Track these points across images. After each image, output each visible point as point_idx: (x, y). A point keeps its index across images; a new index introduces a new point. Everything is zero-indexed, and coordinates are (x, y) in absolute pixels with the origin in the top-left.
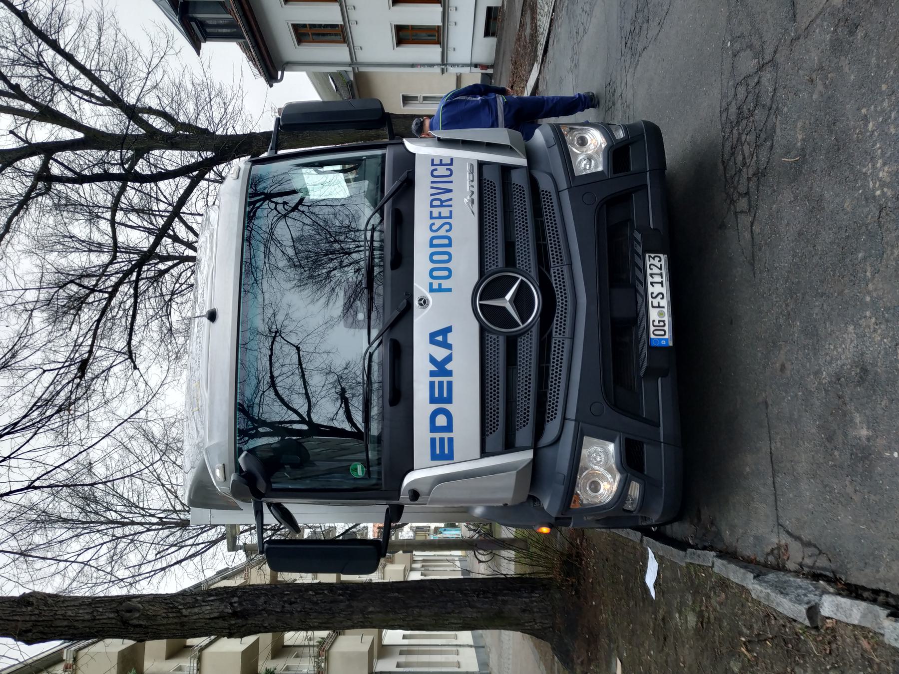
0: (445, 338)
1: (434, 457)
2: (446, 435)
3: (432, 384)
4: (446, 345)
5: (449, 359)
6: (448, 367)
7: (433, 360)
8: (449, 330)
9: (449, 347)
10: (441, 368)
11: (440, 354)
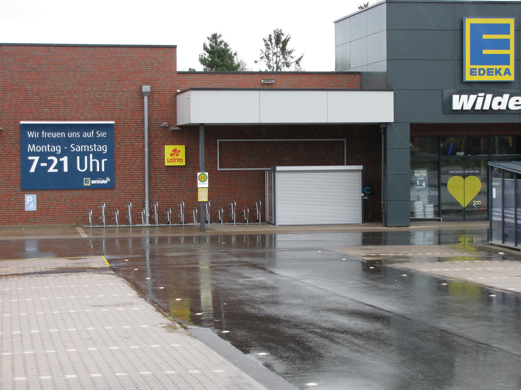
0: (507, 73)
1: (471, 69)
2: (477, 73)
3: (493, 69)
5: (500, 75)
6: (498, 74)
7: (500, 69)
8: (510, 75)
9: (505, 75)
10: (498, 72)
11: (502, 72)
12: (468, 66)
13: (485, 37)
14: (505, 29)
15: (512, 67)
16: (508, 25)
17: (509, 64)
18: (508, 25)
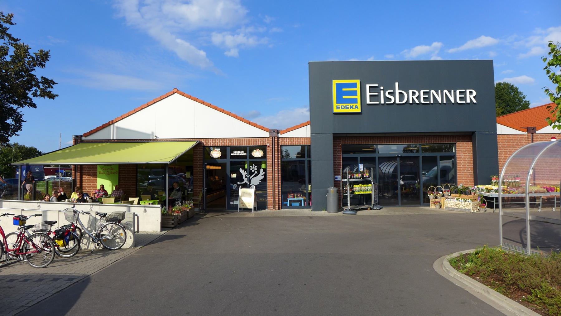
2: (340, 108)
5: (353, 108)
6: (352, 108)
7: (353, 106)
8: (358, 108)
9: (355, 109)
10: (351, 107)
11: (354, 107)
12: (335, 104)
13: (344, 89)
14: (354, 85)
15: (359, 104)
16: (356, 83)
17: (357, 103)
18: (356, 83)
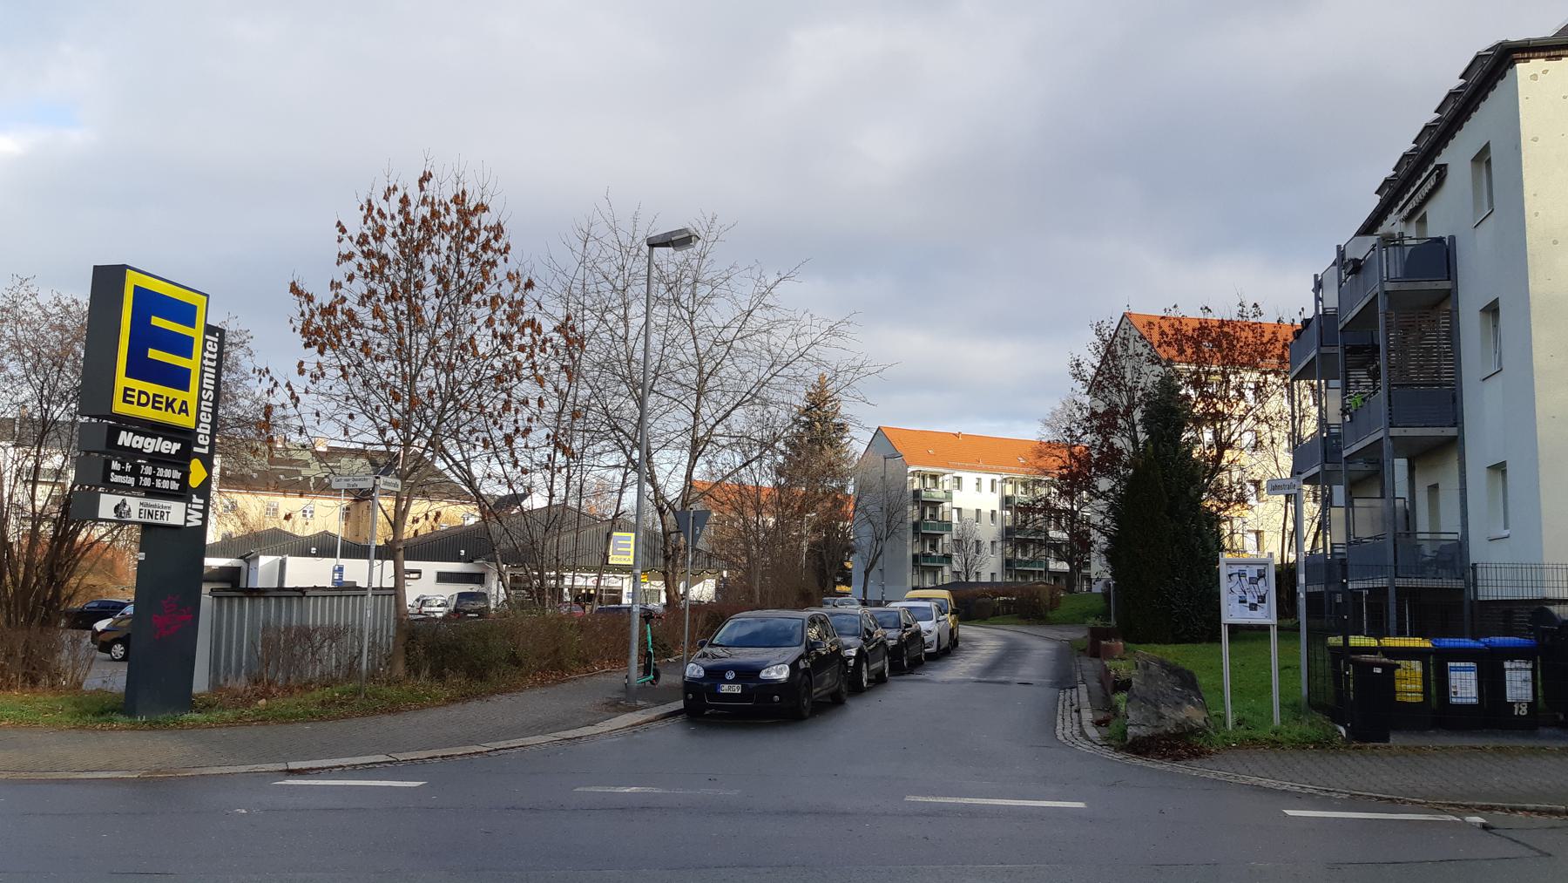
1: (126, 389)
2: (135, 400)
4: (181, 411)
5: (174, 411)
6: (170, 409)
7: (174, 400)
8: (187, 415)
10: (169, 405)
11: (177, 406)
